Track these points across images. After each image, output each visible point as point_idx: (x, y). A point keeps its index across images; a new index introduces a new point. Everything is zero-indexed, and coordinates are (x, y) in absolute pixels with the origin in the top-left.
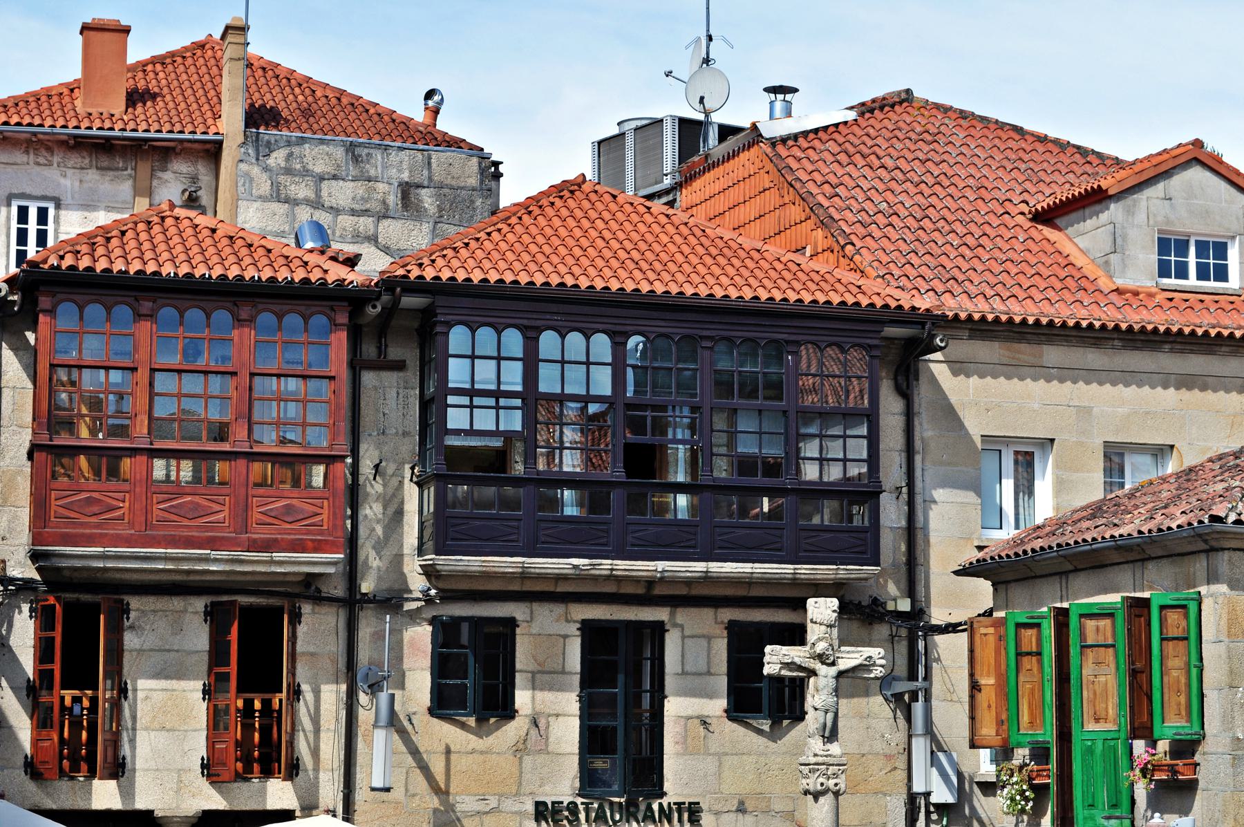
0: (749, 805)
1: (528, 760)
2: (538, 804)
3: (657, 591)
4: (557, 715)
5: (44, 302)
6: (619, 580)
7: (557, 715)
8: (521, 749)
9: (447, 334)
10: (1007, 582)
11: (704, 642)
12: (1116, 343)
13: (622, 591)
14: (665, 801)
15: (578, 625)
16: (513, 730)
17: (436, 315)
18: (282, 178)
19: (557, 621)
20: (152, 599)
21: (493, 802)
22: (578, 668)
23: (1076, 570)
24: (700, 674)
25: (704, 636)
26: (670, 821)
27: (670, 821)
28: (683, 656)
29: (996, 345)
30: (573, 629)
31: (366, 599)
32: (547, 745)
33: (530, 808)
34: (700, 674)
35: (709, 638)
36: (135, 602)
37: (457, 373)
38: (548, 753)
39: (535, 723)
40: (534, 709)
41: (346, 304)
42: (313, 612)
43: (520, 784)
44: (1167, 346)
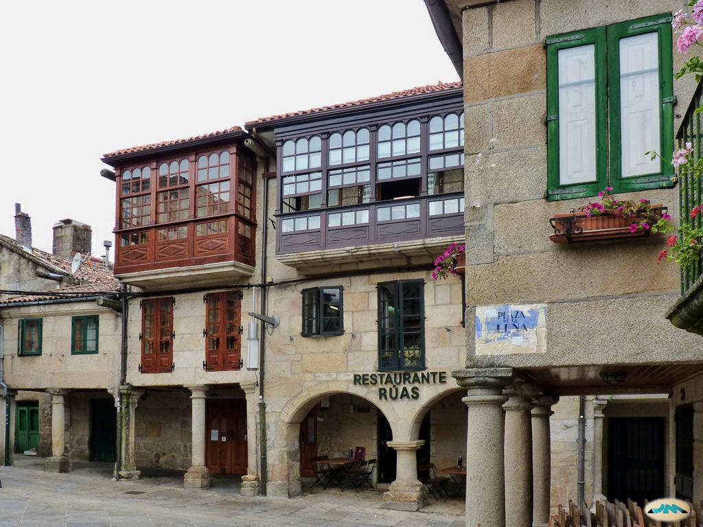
1: (351, 355)
2: (355, 376)
3: (414, 262)
4: (366, 332)
7: (366, 332)
8: (347, 350)
13: (394, 265)
14: (425, 373)
15: (376, 286)
16: (343, 341)
19: (364, 284)
20: (184, 295)
22: (376, 307)
24: (446, 305)
26: (428, 381)
27: (428, 381)
31: (271, 284)
32: (361, 346)
34: (446, 305)
36: (177, 297)
38: (362, 351)
39: (353, 336)
42: (248, 293)
43: (347, 367)
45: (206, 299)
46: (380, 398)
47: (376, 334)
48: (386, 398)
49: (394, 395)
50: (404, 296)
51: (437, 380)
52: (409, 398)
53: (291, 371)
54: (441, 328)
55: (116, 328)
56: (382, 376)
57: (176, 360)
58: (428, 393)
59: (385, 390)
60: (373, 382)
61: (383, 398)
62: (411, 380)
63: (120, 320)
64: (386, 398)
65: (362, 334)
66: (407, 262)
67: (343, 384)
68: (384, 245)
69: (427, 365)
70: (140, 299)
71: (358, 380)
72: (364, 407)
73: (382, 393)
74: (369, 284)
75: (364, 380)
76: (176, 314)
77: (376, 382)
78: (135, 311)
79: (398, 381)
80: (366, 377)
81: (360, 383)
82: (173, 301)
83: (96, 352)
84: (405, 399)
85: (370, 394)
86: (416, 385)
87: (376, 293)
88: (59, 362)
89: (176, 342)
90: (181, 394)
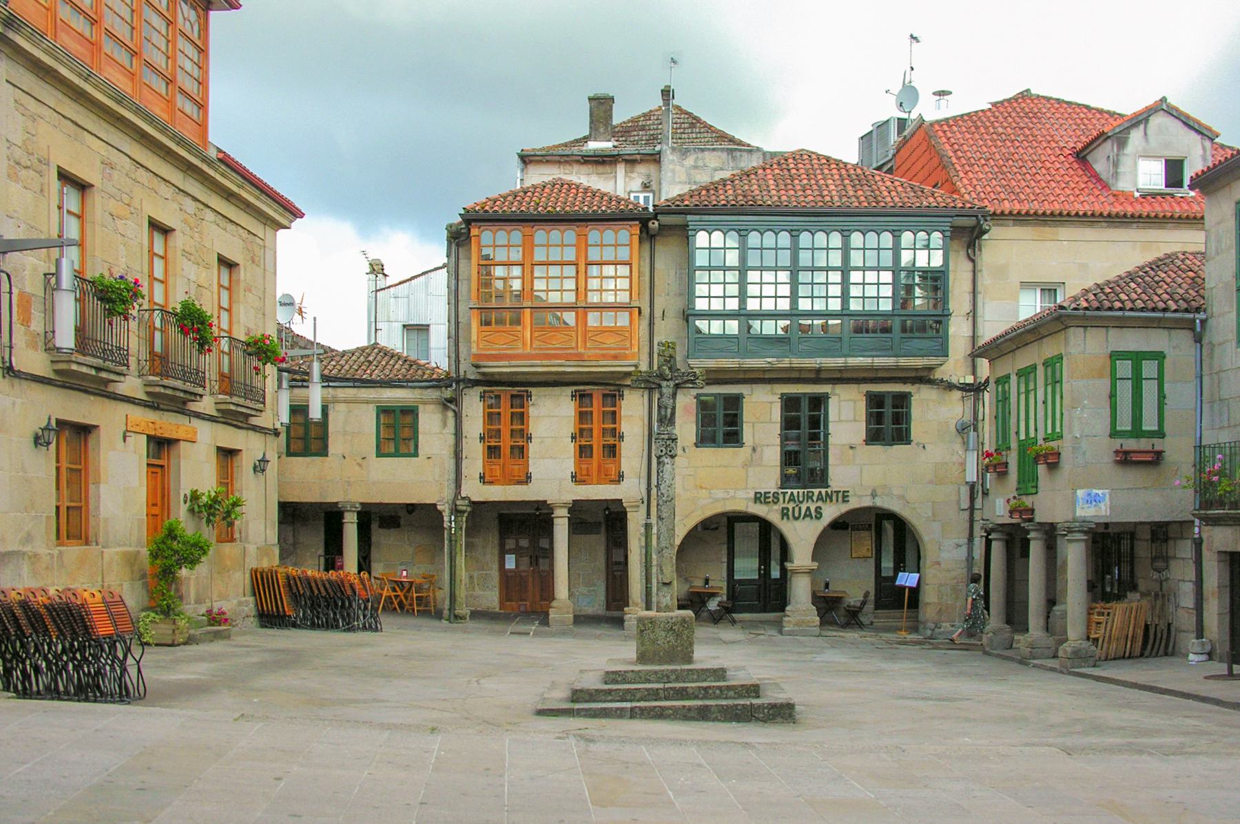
0: (879, 492)
1: (750, 469)
2: (756, 493)
3: (823, 375)
5: (474, 232)
6: (800, 370)
7: (768, 446)
8: (746, 466)
9: (694, 236)
10: (993, 359)
11: (852, 404)
12: (1103, 224)
14: (829, 490)
16: (742, 453)
17: (688, 226)
18: (692, 172)
21: (732, 493)
23: (1018, 348)
25: (851, 400)
26: (831, 501)
27: (831, 501)
28: (839, 412)
29: (1029, 229)
30: (776, 399)
33: (752, 495)
34: (850, 421)
35: (855, 402)
36: (534, 390)
37: (701, 259)
39: (754, 450)
40: (754, 442)
41: (637, 223)
42: (630, 394)
44: (1135, 225)
46: (783, 519)
47: (779, 448)
48: (788, 518)
49: (797, 515)
50: (820, 416)
51: (840, 499)
52: (812, 518)
53: (684, 487)
54: (845, 445)
55: (445, 424)
56: (784, 494)
58: (831, 512)
59: (788, 509)
60: (775, 500)
61: (785, 518)
62: (815, 498)
63: (450, 414)
64: (788, 518)
65: (764, 448)
66: (818, 376)
67: (741, 502)
68: (807, 360)
69: (830, 483)
70: (481, 389)
71: (759, 498)
72: (766, 527)
73: (784, 514)
74: (772, 394)
75: (766, 498)
76: (532, 411)
77: (778, 499)
78: (474, 407)
79: (801, 499)
80: (767, 495)
81: (761, 502)
83: (416, 455)
84: (808, 519)
85: (771, 513)
86: (820, 504)
87: (780, 404)
88: (357, 468)
89: (533, 448)
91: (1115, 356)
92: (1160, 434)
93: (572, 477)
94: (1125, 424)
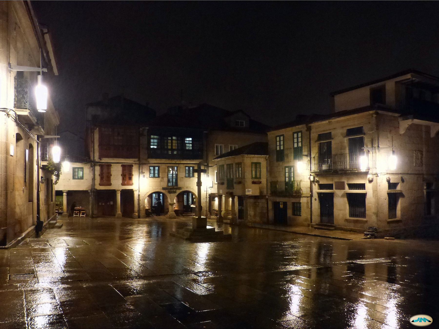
2: (163, 188)
33: (162, 188)
36: (112, 164)
45: (122, 166)
57: (112, 182)
76: (112, 169)
82: (111, 165)
90: (114, 192)
91: (252, 163)
92: (260, 178)
93: (121, 184)
94: (254, 176)
